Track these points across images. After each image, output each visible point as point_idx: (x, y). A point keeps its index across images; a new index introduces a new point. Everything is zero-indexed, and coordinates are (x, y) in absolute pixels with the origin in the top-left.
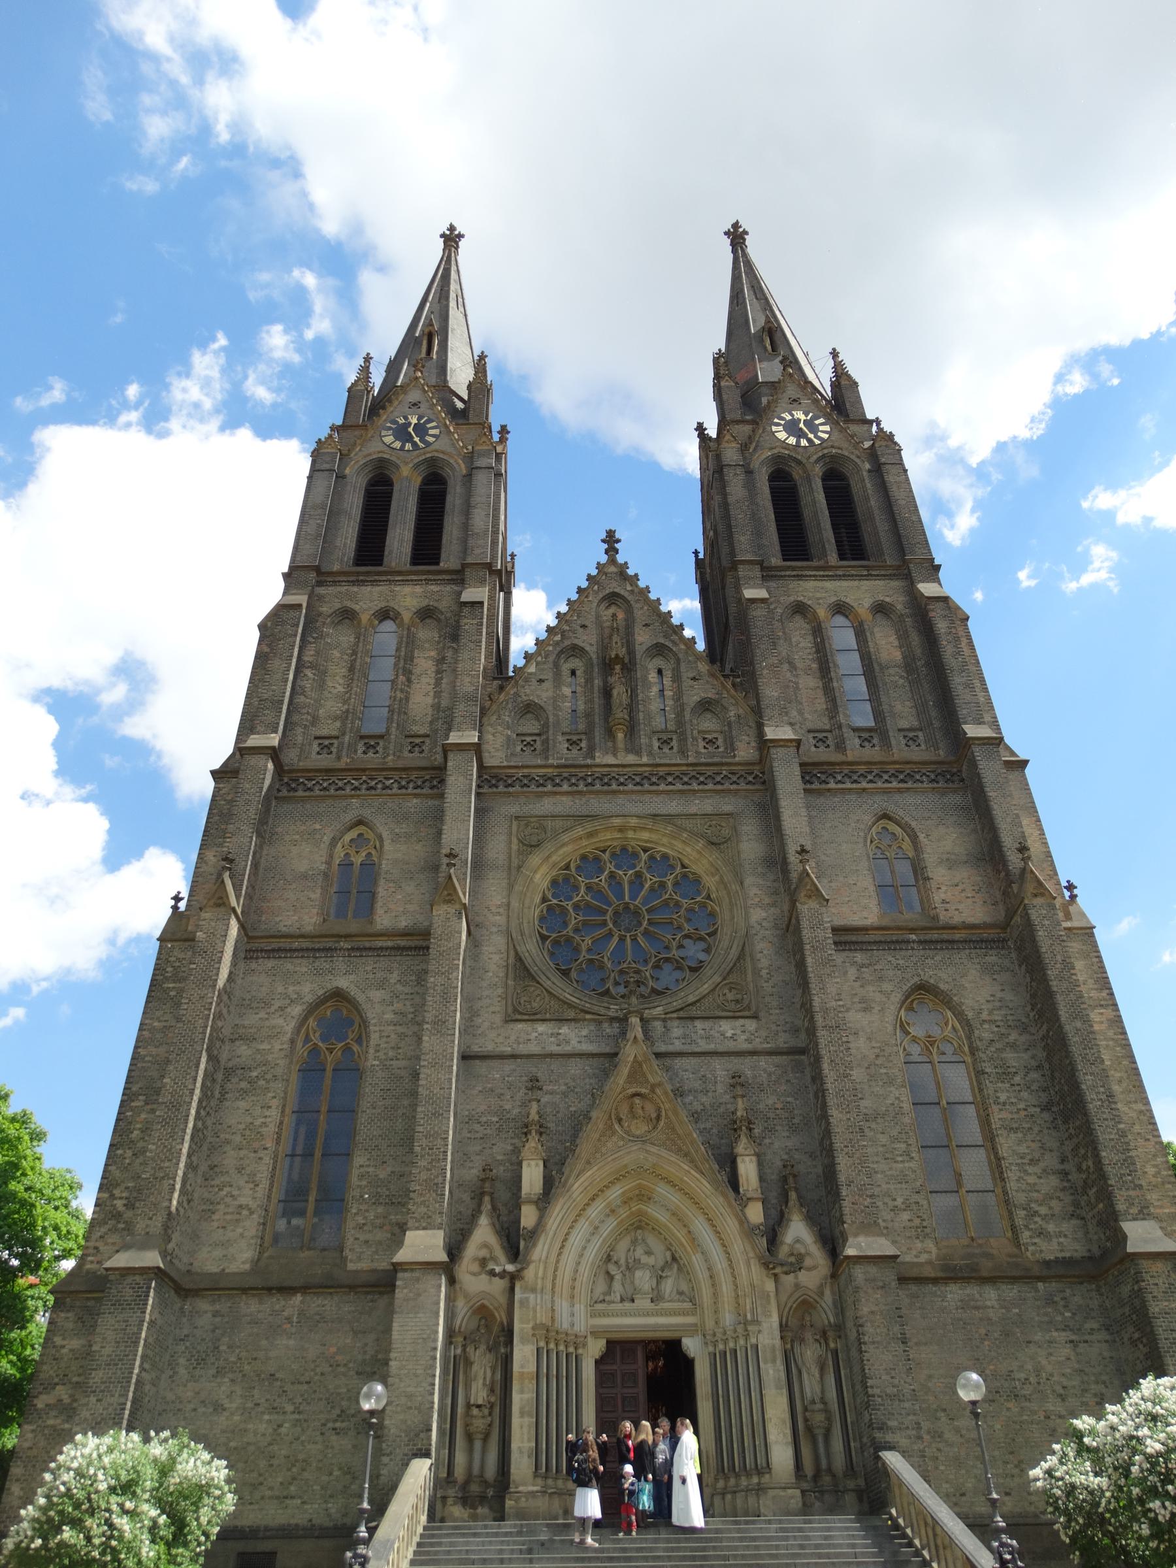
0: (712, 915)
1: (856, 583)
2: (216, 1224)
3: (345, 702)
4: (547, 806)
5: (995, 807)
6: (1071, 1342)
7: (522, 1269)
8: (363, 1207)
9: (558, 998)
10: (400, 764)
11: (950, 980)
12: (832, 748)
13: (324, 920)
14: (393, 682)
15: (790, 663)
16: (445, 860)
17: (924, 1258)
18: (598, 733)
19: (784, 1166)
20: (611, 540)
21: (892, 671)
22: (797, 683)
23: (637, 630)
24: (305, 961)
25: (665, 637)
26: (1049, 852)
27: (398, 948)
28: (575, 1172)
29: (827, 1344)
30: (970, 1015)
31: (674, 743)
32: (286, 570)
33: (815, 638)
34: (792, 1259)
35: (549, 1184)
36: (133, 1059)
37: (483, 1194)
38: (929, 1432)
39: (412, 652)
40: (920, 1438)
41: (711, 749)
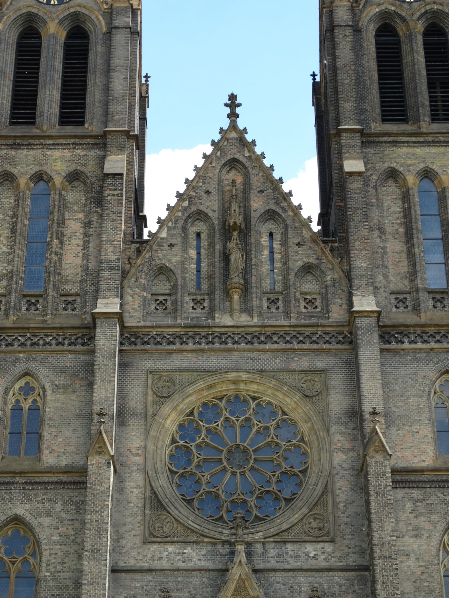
0: (305, 454)
1: (442, 149)
3: (10, 262)
9: (184, 525)
12: (410, 308)
22: (384, 248)
25: (277, 203)
27: (61, 483)
33: (404, 203)
39: (63, 215)
41: (310, 309)
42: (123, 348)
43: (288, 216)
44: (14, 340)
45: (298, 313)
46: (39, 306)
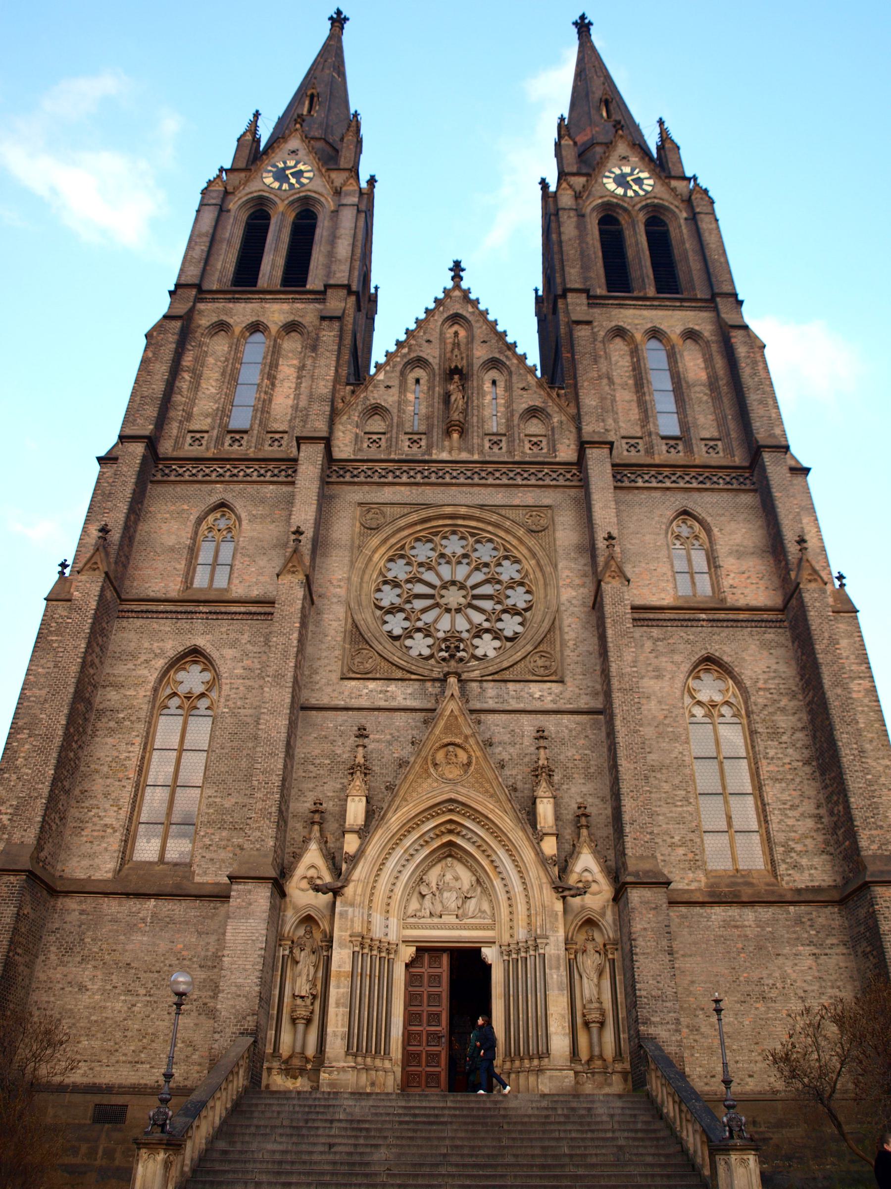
1: (670, 313)
2: (85, 839)
4: (387, 494)
5: (780, 505)
6: (814, 954)
7: (343, 887)
8: (210, 831)
9: (388, 660)
10: (260, 455)
11: (733, 653)
12: (642, 452)
13: (187, 588)
14: (258, 385)
15: (609, 378)
16: (293, 537)
17: (693, 886)
18: (436, 434)
19: (579, 808)
20: (457, 268)
21: (697, 389)
23: (475, 346)
24: (169, 621)
25: (500, 352)
26: (824, 547)
27: (251, 613)
28: (394, 808)
29: (606, 955)
30: (748, 683)
31: (503, 444)
32: (172, 288)
33: (632, 358)
34: (580, 885)
35: (371, 814)
36: (20, 698)
37: (313, 823)
38: (688, 1027)
39: (277, 361)
40: (678, 1031)
42: (330, 480)
43: (512, 364)
44: (212, 471)
45: (522, 452)
46: (244, 442)
